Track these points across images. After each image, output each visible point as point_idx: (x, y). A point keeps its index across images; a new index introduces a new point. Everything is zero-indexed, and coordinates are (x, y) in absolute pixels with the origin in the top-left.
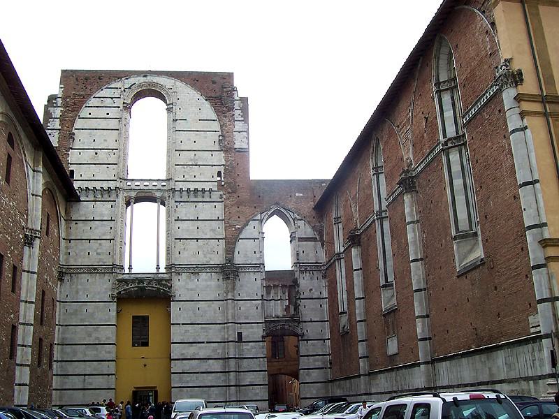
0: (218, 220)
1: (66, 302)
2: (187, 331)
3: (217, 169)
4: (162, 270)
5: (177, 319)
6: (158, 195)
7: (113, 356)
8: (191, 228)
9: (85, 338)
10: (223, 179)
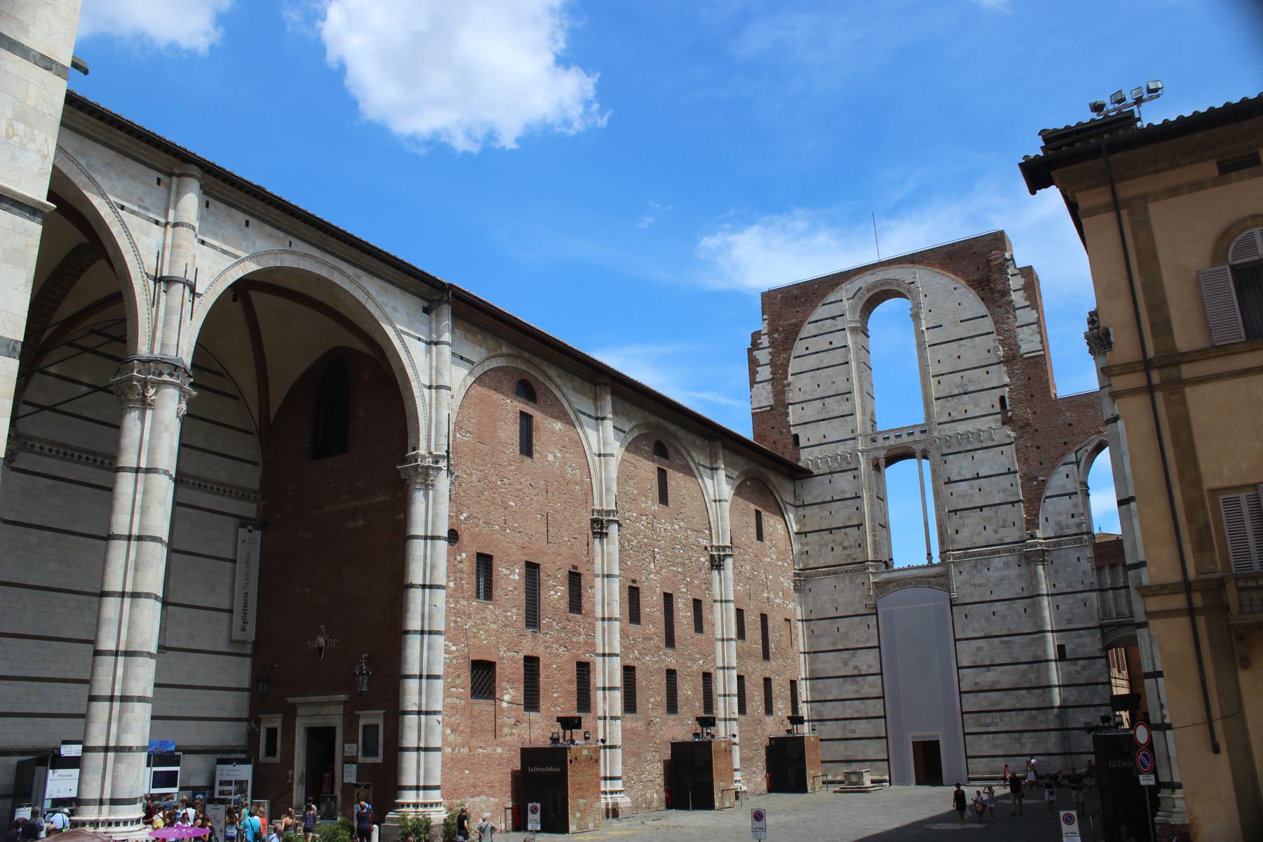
0: (1009, 472)
1: (811, 620)
2: (979, 649)
3: (998, 393)
4: (936, 560)
5: (964, 632)
6: (918, 448)
7: (877, 691)
8: (971, 492)
9: (839, 668)
10: (1008, 408)
